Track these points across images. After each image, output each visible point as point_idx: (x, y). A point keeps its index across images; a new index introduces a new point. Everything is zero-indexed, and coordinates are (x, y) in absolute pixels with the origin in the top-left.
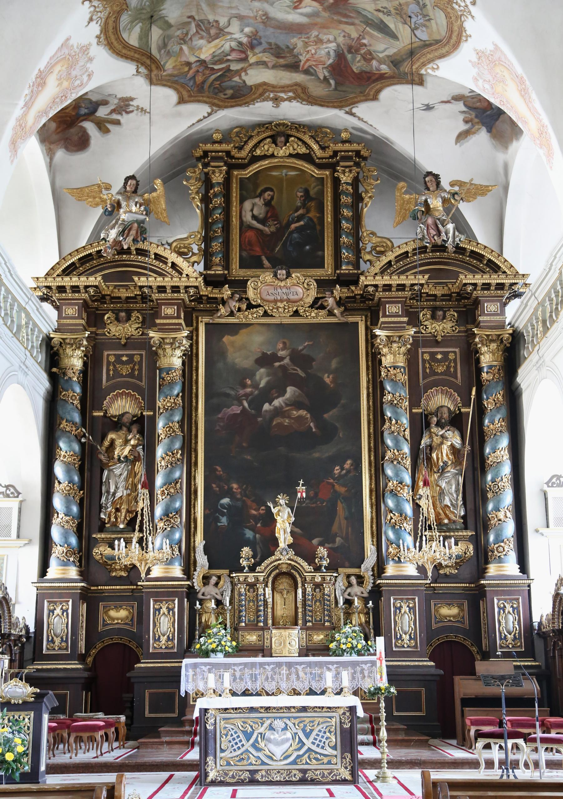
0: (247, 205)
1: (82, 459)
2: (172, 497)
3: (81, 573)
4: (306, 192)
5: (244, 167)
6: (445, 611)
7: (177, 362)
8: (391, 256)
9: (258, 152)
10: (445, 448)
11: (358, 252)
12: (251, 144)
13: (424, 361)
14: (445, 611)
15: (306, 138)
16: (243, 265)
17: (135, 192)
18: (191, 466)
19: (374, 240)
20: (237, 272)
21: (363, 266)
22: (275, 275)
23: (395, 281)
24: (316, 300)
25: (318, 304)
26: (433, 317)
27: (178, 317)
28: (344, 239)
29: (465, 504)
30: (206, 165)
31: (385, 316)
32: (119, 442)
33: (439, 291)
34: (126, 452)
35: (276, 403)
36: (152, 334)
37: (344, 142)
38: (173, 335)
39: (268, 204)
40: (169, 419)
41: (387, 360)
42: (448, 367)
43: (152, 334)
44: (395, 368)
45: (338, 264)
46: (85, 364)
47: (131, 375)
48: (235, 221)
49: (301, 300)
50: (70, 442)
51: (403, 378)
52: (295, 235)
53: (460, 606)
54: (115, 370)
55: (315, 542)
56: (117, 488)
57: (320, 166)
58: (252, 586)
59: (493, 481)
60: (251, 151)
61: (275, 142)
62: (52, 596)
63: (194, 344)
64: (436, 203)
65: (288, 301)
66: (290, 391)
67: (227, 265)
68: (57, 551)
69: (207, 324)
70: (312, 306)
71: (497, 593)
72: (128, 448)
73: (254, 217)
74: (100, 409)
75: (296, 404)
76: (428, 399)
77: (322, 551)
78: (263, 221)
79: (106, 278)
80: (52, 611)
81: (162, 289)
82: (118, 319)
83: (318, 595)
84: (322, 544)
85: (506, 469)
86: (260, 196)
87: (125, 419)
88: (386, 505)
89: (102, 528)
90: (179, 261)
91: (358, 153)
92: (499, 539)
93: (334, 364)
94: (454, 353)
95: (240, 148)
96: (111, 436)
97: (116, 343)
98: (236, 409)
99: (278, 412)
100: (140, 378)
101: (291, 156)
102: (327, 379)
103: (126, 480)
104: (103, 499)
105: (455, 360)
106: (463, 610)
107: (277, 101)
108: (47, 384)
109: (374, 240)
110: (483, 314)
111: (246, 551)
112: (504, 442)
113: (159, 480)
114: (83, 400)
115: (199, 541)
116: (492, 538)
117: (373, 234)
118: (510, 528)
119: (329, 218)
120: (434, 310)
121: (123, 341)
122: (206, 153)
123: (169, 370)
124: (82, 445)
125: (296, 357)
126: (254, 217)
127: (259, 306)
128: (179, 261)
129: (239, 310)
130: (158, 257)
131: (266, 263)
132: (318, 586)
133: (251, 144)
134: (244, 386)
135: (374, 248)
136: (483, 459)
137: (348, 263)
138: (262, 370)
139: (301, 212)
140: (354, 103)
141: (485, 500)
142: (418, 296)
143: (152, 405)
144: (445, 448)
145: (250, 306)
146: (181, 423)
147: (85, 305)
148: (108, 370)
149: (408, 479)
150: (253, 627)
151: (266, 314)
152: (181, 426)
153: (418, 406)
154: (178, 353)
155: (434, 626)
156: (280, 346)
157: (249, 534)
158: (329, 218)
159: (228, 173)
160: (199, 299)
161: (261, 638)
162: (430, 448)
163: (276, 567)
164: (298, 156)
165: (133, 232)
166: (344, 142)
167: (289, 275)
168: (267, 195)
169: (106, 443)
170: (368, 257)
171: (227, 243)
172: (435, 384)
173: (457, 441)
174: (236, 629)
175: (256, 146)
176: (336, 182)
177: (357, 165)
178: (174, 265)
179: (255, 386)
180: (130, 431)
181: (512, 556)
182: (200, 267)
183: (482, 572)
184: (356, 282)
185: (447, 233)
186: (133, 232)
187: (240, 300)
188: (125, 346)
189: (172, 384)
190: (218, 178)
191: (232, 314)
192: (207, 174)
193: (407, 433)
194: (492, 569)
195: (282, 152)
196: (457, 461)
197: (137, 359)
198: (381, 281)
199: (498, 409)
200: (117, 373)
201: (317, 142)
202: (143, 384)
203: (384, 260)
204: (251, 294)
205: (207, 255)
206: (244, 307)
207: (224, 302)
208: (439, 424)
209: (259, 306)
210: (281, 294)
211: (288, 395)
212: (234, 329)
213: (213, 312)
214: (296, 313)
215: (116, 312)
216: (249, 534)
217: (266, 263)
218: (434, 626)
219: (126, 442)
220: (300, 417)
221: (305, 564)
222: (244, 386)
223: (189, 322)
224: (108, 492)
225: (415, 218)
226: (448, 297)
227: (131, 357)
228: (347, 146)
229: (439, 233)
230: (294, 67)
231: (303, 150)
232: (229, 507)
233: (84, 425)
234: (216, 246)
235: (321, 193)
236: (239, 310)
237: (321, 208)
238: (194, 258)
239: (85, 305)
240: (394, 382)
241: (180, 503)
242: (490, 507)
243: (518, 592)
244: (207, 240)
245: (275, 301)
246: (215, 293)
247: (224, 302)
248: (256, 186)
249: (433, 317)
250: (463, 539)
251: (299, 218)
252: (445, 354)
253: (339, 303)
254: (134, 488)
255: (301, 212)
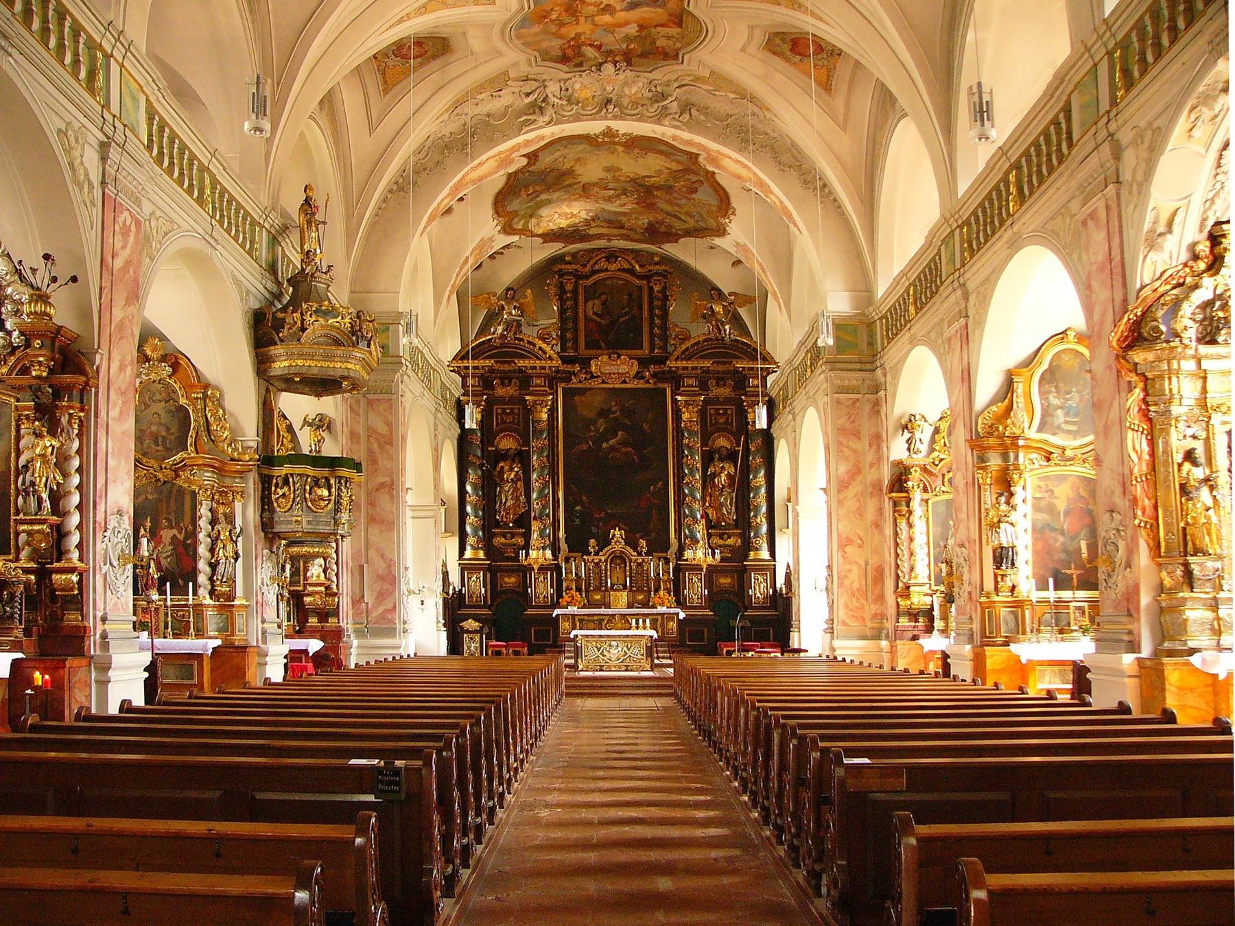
0: (590, 304)
1: (483, 481)
2: (544, 507)
3: (486, 554)
4: (630, 295)
5: (587, 277)
6: (722, 581)
7: (545, 416)
8: (688, 344)
9: (597, 267)
10: (723, 476)
11: (665, 338)
12: (592, 263)
13: (711, 415)
14: (722, 581)
15: (629, 258)
16: (587, 347)
17: (513, 298)
18: (555, 485)
19: (677, 329)
20: (583, 351)
21: (670, 349)
22: (610, 357)
23: (690, 364)
24: (638, 373)
25: (639, 376)
26: (717, 384)
27: (545, 386)
28: (656, 331)
29: (736, 512)
30: (561, 276)
31: (683, 386)
32: (507, 468)
33: (721, 368)
34: (512, 476)
35: (611, 442)
36: (527, 398)
37: (656, 264)
38: (542, 398)
39: (604, 304)
40: (540, 454)
41: (685, 416)
42: (728, 419)
43: (527, 398)
44: (691, 422)
45: (652, 350)
46: (482, 416)
47: (513, 422)
48: (581, 315)
49: (628, 373)
50: (475, 471)
51: (697, 428)
52: (623, 326)
53: (732, 578)
54: (502, 418)
55: (638, 535)
56: (507, 500)
57: (640, 277)
58: (597, 564)
59: (754, 498)
60: (592, 267)
61: (607, 260)
62: (469, 569)
63: (555, 401)
64: (718, 309)
65: (618, 373)
66: (620, 433)
67: (576, 350)
68: (471, 540)
69: (563, 389)
70: (634, 377)
71: (754, 570)
72: (513, 474)
73: (595, 313)
74: (493, 446)
75: (624, 443)
76: (714, 441)
77: (643, 543)
78: (600, 316)
79: (496, 362)
80: (469, 578)
81: (535, 368)
82: (503, 384)
83: (640, 570)
84: (642, 537)
85: (763, 490)
86: (599, 298)
87: (511, 452)
88: (684, 512)
89: (497, 525)
90: (544, 346)
91: (666, 271)
92: (756, 536)
93: (650, 416)
94: (731, 409)
95: (584, 266)
96: (501, 464)
97: (502, 401)
98: (585, 447)
99: (612, 448)
100: (518, 424)
101: (619, 270)
102: (646, 427)
103: (512, 494)
104: (497, 507)
105: (732, 415)
106: (733, 580)
107: (609, 240)
108: (459, 431)
109: (677, 329)
110: (749, 387)
111: (592, 542)
112: (762, 473)
113: (534, 496)
114: (482, 441)
115: (562, 534)
116: (752, 534)
117: (677, 326)
118: (764, 529)
119: (646, 314)
120: (718, 379)
121: (507, 399)
122: (561, 270)
123: (539, 422)
124: (483, 471)
125: (626, 412)
126: (595, 313)
127: (598, 377)
128: (544, 346)
129: (586, 379)
130: (529, 342)
131: (603, 345)
132: (639, 565)
133: (592, 263)
134: (590, 431)
135: (676, 336)
136: (749, 483)
137: (659, 348)
138: (601, 420)
139: (627, 310)
140: (663, 243)
141: (749, 510)
142: (706, 371)
143: (527, 443)
144: (723, 476)
145: (593, 377)
146: (548, 457)
147: (482, 377)
148: (497, 419)
149: (698, 496)
150: (598, 589)
151: (603, 382)
152: (548, 459)
153: (707, 446)
154: (545, 410)
155: (715, 590)
156: (613, 403)
157: (594, 530)
158: (646, 314)
159: (576, 282)
160: (558, 371)
161: (604, 597)
162: (714, 475)
163: (612, 553)
164: (624, 270)
165: (513, 329)
166: (656, 264)
167: (619, 357)
168: (603, 297)
169: (498, 469)
170: (672, 342)
171: (576, 330)
172: (719, 430)
173: (732, 471)
174: (587, 591)
175: (595, 263)
176: (651, 289)
177: (665, 277)
178: (540, 348)
179: (597, 430)
180: (514, 462)
181: (765, 546)
182: (558, 349)
183: (747, 555)
184: (665, 364)
185: (725, 331)
186: (513, 329)
187: (586, 373)
188: (507, 404)
189: (541, 432)
190: (569, 287)
191: (580, 382)
192: (562, 282)
193: (699, 465)
194: (752, 555)
195: (613, 267)
196: (731, 485)
197: (516, 411)
198: (679, 364)
199: (757, 451)
200: (503, 422)
201: (637, 262)
202: (521, 428)
203: (684, 347)
204: (593, 369)
205: (563, 339)
206: (588, 377)
207: (575, 374)
208: (721, 460)
209: (598, 377)
210: (614, 369)
211: (618, 437)
212: (582, 392)
213: (569, 380)
214: (624, 382)
215: (502, 379)
216: (594, 530)
217: (603, 345)
218: (715, 590)
219: (511, 469)
220: (628, 452)
221: (631, 551)
222: (590, 431)
223: (551, 387)
224: (501, 502)
225: (705, 318)
226: (728, 372)
227: (512, 410)
228: (658, 267)
229: (720, 330)
230: (622, 227)
231: (626, 266)
232: (581, 512)
233: (483, 458)
234: (569, 335)
235: (640, 298)
236: (586, 379)
237: (640, 308)
238: (554, 342)
239: (482, 377)
240: (690, 432)
241: (550, 511)
242: (752, 514)
243: (767, 570)
244: (563, 329)
245: (610, 374)
246: (569, 368)
247: (575, 374)
248: (595, 292)
249: (717, 384)
250: (733, 534)
251: (626, 314)
252: (725, 410)
253: (654, 376)
254: (518, 498)
255: (627, 310)
